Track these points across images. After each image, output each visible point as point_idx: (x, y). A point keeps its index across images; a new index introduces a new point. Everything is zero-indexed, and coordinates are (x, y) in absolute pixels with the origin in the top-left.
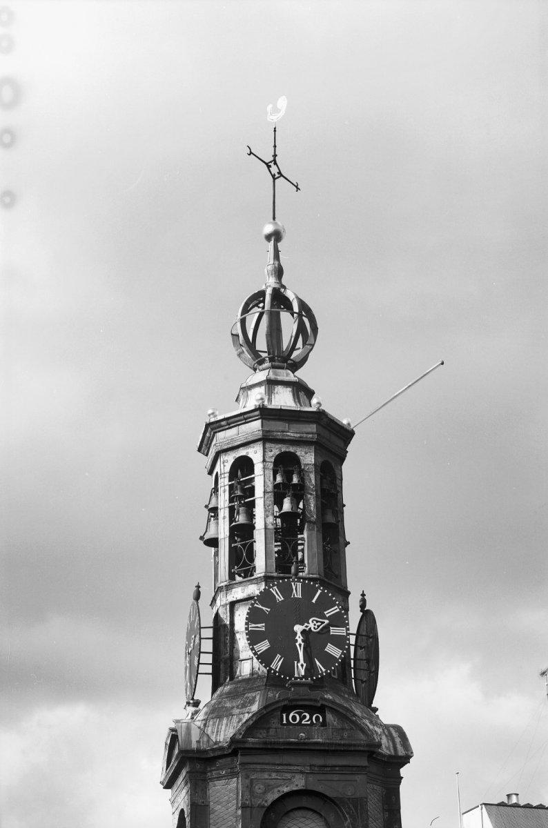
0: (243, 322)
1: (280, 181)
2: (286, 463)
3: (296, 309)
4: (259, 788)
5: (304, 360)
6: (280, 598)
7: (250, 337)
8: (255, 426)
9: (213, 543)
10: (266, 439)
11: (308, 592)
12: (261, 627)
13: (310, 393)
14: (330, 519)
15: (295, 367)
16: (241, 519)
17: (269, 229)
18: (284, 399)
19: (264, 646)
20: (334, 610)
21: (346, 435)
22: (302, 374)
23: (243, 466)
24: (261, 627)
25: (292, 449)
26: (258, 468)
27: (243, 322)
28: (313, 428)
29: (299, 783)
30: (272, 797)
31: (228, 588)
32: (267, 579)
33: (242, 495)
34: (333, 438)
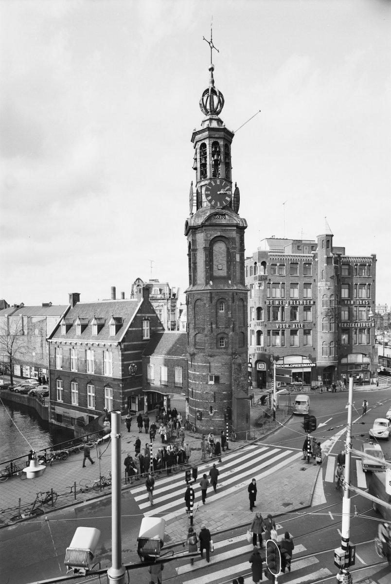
0: (203, 99)
1: (213, 49)
2: (215, 145)
3: (218, 95)
4: (209, 235)
5: (220, 111)
6: (214, 184)
7: (205, 104)
8: (207, 133)
9: (195, 169)
10: (210, 137)
11: (221, 182)
12: (209, 192)
13: (222, 122)
14: (227, 161)
15: (218, 113)
16: (203, 162)
17: (210, 67)
18: (214, 124)
19: (210, 198)
20: (229, 187)
21: (232, 135)
22: (220, 116)
23: (203, 146)
24: (209, 192)
25: (217, 140)
26: (208, 146)
27: (203, 99)
28: (222, 133)
29: (219, 234)
30: (212, 238)
31: (200, 182)
32: (210, 179)
33: (203, 155)
34: (228, 136)
